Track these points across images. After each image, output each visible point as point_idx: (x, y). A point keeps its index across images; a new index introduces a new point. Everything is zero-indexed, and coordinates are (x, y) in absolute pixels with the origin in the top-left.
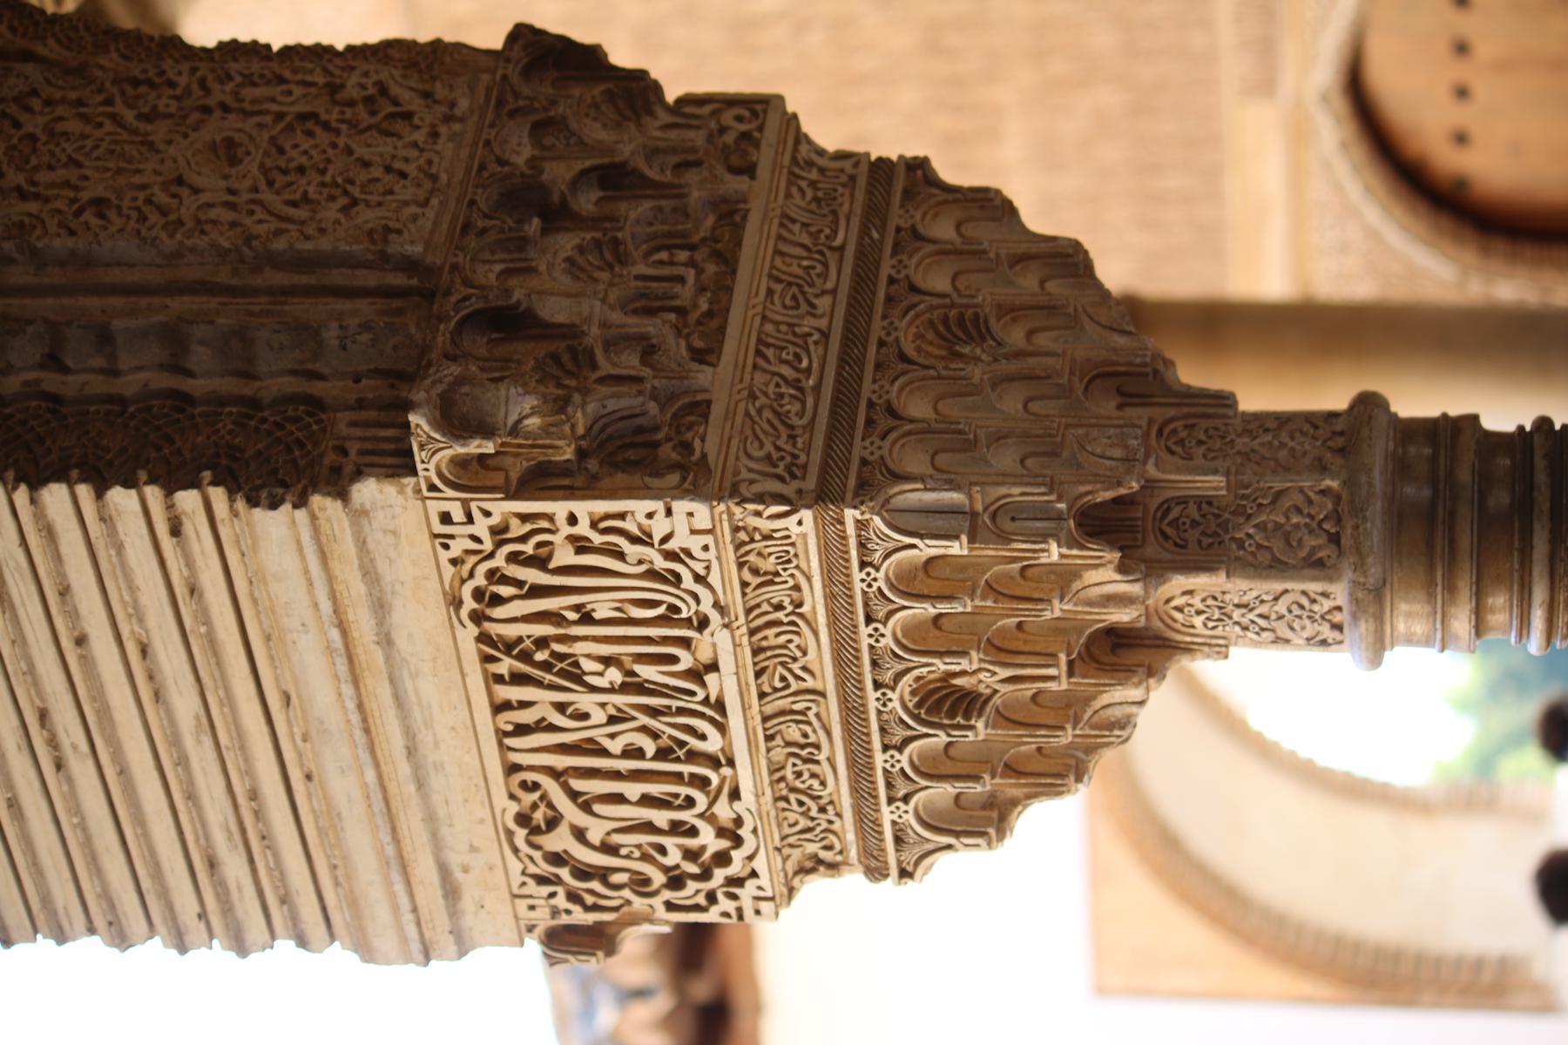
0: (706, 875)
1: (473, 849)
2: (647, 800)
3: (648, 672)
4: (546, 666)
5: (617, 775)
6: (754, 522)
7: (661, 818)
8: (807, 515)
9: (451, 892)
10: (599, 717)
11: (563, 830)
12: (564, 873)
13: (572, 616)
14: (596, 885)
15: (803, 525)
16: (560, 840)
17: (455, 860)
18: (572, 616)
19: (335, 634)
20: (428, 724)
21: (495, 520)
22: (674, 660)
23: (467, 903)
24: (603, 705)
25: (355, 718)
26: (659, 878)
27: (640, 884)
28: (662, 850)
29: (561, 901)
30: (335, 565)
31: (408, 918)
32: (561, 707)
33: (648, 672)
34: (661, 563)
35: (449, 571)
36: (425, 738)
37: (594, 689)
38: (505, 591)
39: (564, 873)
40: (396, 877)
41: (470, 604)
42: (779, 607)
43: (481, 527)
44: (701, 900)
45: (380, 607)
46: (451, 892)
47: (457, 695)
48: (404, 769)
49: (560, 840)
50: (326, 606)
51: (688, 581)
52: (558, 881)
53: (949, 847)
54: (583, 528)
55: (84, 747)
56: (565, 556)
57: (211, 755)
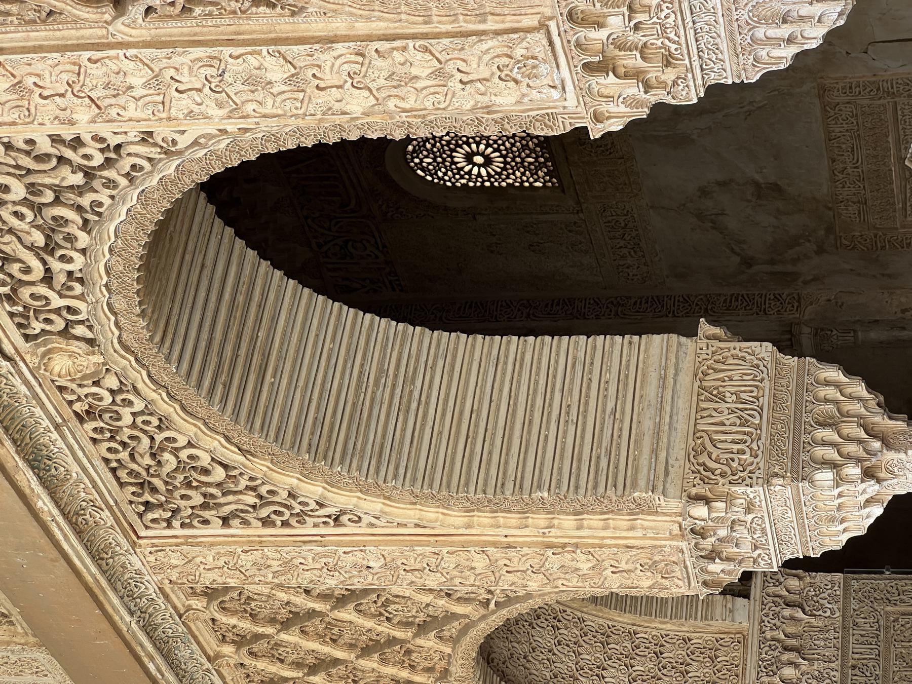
0: (744, 471)
1: (677, 459)
2: (733, 442)
3: (743, 396)
4: (716, 396)
5: (725, 432)
6: (783, 360)
7: (735, 447)
8: (796, 358)
9: (667, 473)
10: (726, 412)
11: (706, 453)
12: (701, 469)
13: (726, 379)
14: (709, 474)
15: (793, 361)
16: (704, 458)
17: (671, 462)
18: (726, 379)
19: (663, 372)
20: (677, 414)
21: (714, 349)
22: (752, 392)
23: (669, 480)
24: (728, 409)
25: (659, 400)
26: (729, 472)
27: (722, 475)
28: (733, 460)
29: (697, 481)
30: (669, 355)
31: (653, 471)
32: (715, 410)
33: (743, 396)
34: (756, 362)
35: (697, 364)
36: (675, 418)
37: (726, 402)
38: (711, 371)
39: (701, 469)
40: (654, 456)
41: (701, 375)
42: (783, 386)
43: (709, 352)
44: (740, 481)
45: (676, 374)
46: (667, 473)
47: (688, 404)
48: (668, 419)
49: (704, 458)
50: (663, 364)
51: (762, 368)
52: (699, 472)
53: (819, 469)
54: (737, 352)
55: (575, 421)
56: (732, 361)
57: (612, 422)
